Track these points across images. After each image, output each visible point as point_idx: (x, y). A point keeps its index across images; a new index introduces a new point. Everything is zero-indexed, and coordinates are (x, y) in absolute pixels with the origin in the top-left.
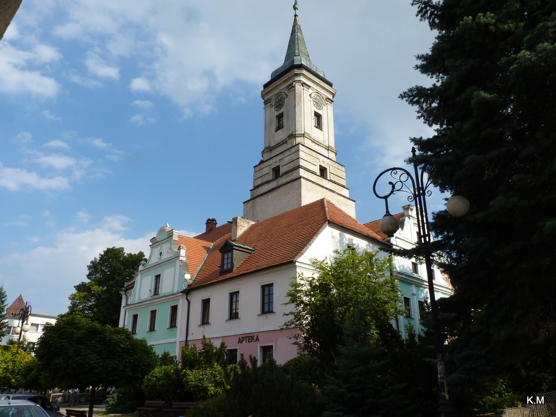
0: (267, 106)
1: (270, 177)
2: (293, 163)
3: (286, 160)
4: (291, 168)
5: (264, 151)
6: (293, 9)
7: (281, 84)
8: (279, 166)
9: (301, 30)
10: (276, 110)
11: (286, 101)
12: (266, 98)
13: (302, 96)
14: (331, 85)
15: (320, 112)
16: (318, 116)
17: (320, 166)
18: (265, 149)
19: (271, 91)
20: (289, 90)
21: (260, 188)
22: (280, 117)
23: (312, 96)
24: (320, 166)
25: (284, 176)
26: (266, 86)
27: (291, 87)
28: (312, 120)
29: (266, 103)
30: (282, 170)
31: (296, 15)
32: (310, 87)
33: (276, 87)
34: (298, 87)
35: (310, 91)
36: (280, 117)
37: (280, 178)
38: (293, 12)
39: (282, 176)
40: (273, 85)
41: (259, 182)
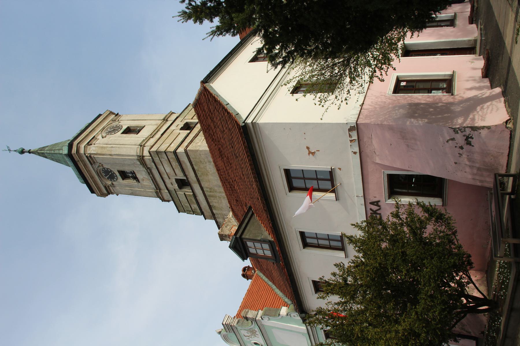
0: (113, 191)
1: (188, 191)
2: (171, 160)
3: (169, 169)
4: (177, 164)
5: (161, 199)
6: (23, 155)
7: (89, 171)
8: (177, 181)
9: (44, 147)
10: (117, 179)
11: (106, 166)
12: (105, 192)
13: (101, 145)
14: (100, 115)
15: (124, 127)
16: (128, 131)
17: (182, 129)
18: (158, 197)
19: (96, 184)
20: (94, 162)
21: (202, 206)
22: (124, 175)
23: (104, 135)
24: (182, 129)
25: (187, 174)
26: (92, 191)
27: (90, 158)
28: (131, 138)
29: (109, 193)
30: (181, 176)
31: (29, 152)
32: (94, 137)
33: (92, 177)
34: (92, 150)
35: (100, 137)
36: (124, 175)
37: (190, 180)
38: (27, 154)
39: (187, 178)
40: (90, 181)
41: (195, 206)
